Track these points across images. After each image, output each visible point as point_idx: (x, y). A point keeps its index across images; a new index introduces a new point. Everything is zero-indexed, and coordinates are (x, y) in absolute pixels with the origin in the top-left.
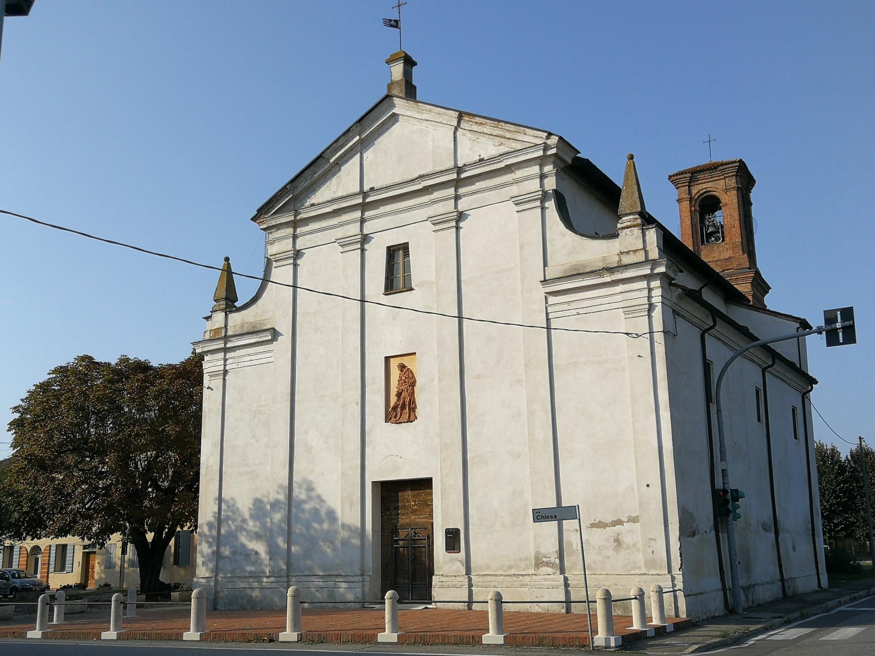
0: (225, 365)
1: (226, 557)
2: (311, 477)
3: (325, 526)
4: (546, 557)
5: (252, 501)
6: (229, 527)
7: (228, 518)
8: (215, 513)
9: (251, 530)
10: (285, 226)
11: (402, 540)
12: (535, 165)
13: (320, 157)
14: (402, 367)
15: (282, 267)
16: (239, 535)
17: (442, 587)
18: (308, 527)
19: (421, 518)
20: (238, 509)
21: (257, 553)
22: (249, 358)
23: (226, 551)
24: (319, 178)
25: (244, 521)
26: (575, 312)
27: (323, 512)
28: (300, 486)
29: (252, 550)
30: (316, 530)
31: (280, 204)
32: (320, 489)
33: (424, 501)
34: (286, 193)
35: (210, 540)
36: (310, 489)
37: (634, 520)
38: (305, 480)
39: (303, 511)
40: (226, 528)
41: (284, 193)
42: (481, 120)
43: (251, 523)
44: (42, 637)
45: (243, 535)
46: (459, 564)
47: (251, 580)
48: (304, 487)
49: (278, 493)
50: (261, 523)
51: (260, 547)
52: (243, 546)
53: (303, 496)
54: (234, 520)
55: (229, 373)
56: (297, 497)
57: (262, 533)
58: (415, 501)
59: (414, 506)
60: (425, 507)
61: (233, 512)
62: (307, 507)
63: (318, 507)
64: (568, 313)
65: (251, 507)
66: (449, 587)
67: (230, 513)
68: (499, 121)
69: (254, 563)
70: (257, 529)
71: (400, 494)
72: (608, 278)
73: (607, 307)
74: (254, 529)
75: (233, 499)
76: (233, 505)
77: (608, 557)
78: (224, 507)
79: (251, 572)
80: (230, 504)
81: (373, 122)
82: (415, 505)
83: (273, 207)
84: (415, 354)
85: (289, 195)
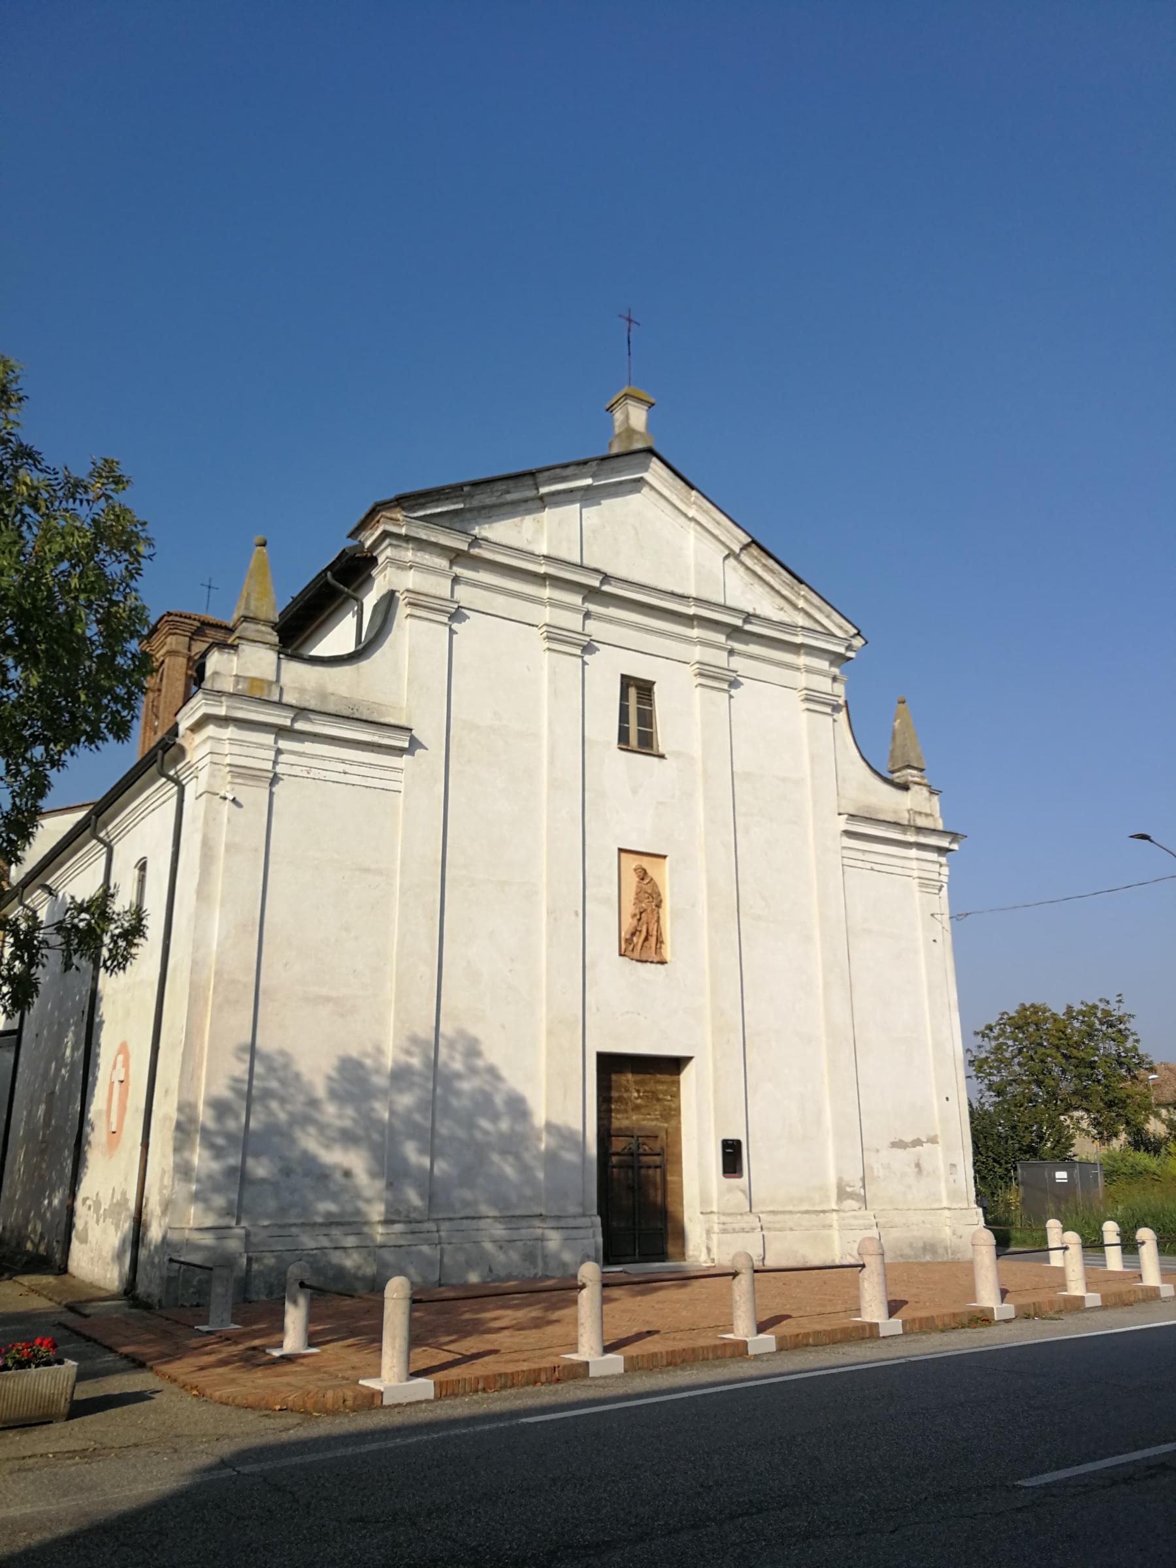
0: (275, 763)
1: (263, 1181)
2: (474, 1030)
3: (504, 1125)
4: (850, 1186)
5: (335, 1062)
6: (270, 1113)
7: (268, 1094)
8: (236, 1080)
9: (329, 1126)
10: (438, 550)
11: (618, 1154)
12: (826, 660)
13: (532, 474)
14: (643, 874)
15: (426, 623)
16: (298, 1133)
17: (724, 1231)
18: (471, 1125)
19: (648, 1119)
20: (297, 1076)
21: (347, 1174)
22: (341, 767)
23: (260, 1169)
24: (514, 503)
25: (313, 1103)
26: (869, 866)
27: (499, 1100)
28: (451, 1045)
29: (335, 1167)
30: (486, 1133)
31: (437, 507)
32: (494, 1054)
33: (653, 1092)
34: (456, 497)
35: (220, 1141)
36: (473, 1050)
37: (933, 1140)
38: (462, 1034)
39: (458, 1094)
40: (262, 1117)
41: (453, 495)
42: (776, 567)
43: (330, 1110)
44: (626, 1371)
45: (309, 1135)
46: (740, 1195)
47: (336, 1232)
48: (460, 1047)
49: (408, 1053)
50: (358, 1110)
51: (355, 1161)
52: (309, 1159)
53: (458, 1065)
54: (283, 1101)
55: (281, 782)
56: (446, 1065)
57: (360, 1132)
58: (638, 1091)
59: (637, 1098)
60: (655, 1102)
61: (283, 1082)
62: (466, 1086)
63: (487, 1088)
64: (860, 864)
65: (334, 1074)
66: (734, 1231)
67: (274, 1084)
68: (801, 582)
69: (334, 1197)
70: (347, 1123)
71: (614, 1077)
72: (911, 838)
73: (899, 871)
74: (338, 1123)
75: (283, 1053)
76: (286, 1066)
77: (910, 1187)
78: (258, 1069)
79: (329, 1214)
80: (276, 1065)
81: (619, 472)
82: (639, 1097)
83: (423, 506)
84: (665, 857)
85: (457, 503)
